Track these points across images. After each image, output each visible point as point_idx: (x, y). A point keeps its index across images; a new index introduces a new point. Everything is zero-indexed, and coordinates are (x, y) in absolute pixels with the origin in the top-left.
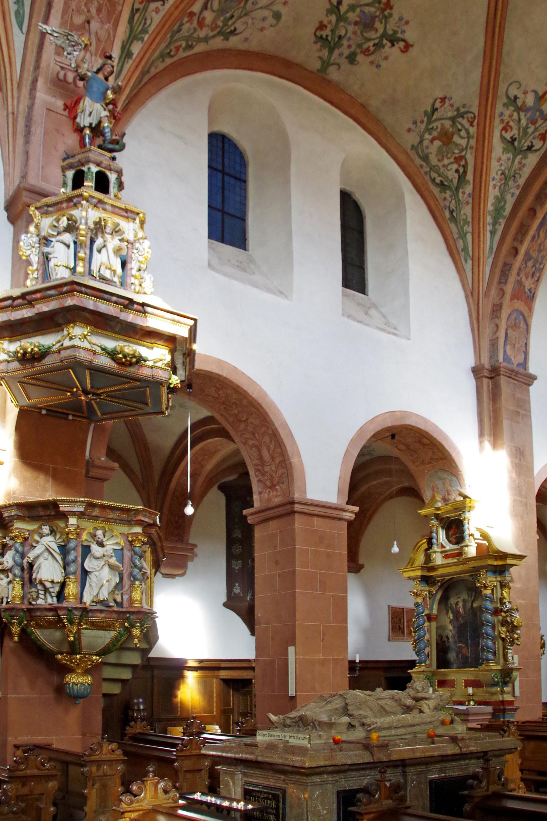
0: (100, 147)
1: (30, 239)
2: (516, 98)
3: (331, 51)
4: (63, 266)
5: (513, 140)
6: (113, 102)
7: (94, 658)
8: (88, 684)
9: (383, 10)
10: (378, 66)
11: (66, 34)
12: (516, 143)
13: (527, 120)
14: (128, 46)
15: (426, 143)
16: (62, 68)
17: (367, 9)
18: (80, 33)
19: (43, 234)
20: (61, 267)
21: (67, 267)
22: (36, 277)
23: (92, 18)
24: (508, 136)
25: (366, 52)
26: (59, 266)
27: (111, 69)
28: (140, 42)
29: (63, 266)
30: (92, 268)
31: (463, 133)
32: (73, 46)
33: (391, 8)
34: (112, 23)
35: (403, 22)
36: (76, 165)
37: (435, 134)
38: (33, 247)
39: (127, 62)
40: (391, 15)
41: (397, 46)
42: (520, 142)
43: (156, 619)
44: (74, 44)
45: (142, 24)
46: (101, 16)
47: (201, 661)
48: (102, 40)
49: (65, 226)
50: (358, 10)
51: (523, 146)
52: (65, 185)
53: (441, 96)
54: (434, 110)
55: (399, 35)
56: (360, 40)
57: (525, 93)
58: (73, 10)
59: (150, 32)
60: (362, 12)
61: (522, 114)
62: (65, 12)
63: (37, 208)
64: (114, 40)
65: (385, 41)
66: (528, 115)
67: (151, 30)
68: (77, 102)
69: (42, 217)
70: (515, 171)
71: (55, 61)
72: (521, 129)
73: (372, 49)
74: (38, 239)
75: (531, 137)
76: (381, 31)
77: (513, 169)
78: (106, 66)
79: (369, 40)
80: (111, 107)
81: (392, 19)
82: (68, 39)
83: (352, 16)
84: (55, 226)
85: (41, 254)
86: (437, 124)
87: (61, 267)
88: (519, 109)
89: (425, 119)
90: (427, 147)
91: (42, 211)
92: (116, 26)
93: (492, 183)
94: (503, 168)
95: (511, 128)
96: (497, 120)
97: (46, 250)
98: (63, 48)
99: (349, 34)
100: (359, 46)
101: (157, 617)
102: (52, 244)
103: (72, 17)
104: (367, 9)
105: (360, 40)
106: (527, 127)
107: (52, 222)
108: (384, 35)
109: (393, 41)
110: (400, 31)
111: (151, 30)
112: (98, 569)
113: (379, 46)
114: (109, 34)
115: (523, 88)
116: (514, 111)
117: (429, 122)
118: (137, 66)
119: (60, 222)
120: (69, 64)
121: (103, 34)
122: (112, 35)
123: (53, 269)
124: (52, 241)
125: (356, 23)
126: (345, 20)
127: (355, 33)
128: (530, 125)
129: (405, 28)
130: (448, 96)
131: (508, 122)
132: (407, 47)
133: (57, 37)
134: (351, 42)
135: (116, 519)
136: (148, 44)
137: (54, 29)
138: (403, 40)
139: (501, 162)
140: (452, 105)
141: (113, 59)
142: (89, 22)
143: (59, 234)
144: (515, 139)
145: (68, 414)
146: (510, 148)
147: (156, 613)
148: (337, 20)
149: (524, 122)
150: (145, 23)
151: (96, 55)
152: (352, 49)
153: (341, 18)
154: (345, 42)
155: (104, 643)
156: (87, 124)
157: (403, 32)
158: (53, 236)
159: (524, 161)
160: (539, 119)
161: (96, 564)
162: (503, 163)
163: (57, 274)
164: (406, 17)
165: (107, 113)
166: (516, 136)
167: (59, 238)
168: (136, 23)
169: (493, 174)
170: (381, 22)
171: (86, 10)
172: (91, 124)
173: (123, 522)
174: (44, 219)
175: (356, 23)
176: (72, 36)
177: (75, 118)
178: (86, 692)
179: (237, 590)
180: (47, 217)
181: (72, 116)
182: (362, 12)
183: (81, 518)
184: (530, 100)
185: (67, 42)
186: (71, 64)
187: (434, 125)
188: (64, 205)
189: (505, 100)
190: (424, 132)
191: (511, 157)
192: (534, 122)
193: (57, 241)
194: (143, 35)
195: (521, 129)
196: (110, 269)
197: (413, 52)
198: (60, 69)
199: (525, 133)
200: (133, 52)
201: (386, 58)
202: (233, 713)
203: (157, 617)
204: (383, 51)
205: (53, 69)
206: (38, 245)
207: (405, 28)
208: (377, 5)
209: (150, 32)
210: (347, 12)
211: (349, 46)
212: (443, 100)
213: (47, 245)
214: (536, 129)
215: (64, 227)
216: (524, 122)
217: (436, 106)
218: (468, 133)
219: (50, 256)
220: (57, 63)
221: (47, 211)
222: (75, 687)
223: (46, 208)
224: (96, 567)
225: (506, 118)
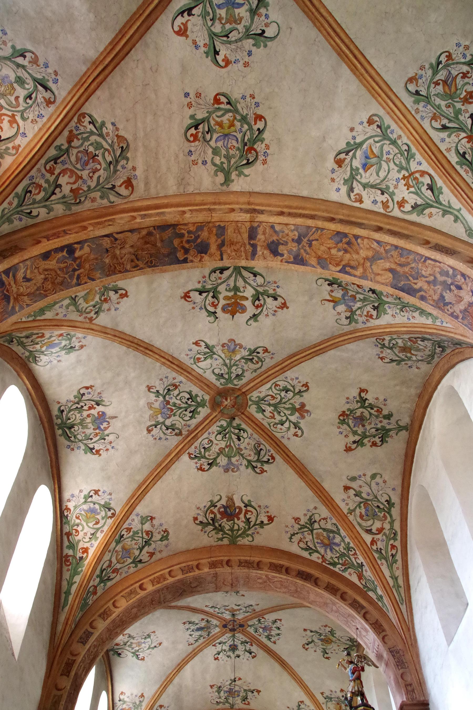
2: (347, 318)
3: (390, 430)
5: (375, 308)
9: (347, 415)
10: (385, 400)
12: (376, 305)
13: (355, 303)
15: (420, 358)
17: (352, 425)
24: (374, 313)
25: (380, 411)
31: (394, 342)
33: (344, 412)
35: (348, 401)
37: (409, 355)
40: (349, 410)
41: (365, 397)
42: (373, 302)
50: (354, 429)
51: (375, 298)
53: (380, 360)
54: (392, 361)
55: (358, 399)
56: (373, 418)
57: (339, 314)
60: (354, 426)
61: (354, 309)
65: (366, 405)
66: (352, 304)
70: (395, 299)
72: (364, 304)
73: (375, 409)
75: (365, 293)
76: (361, 410)
77: (394, 301)
79: (371, 414)
81: (351, 408)
83: (360, 430)
86: (401, 355)
88: (353, 313)
89: (403, 363)
90: (422, 357)
93: (412, 321)
94: (398, 311)
95: (368, 312)
96: (368, 325)
99: (373, 426)
100: (377, 417)
104: (352, 425)
105: (373, 418)
106: (361, 300)
108: (362, 407)
109: (363, 401)
110: (355, 400)
113: (371, 406)
115: (338, 317)
116: (356, 315)
117: (403, 360)
125: (363, 426)
126: (364, 433)
127: (370, 423)
128: (358, 299)
129: (351, 398)
130: (377, 357)
131: (365, 316)
132: (362, 391)
134: (377, 422)
138: (360, 394)
139: (394, 314)
140: (382, 352)
144: (373, 306)
146: (381, 308)
148: (366, 438)
149: (359, 305)
152: (382, 419)
153: (364, 436)
154: (379, 426)
157: (354, 397)
159: (385, 294)
160: (349, 295)
162: (394, 312)
164: (344, 401)
166: (371, 306)
169: (405, 320)
170: (356, 413)
175: (363, 426)
182: (354, 426)
184: (341, 308)
187: (403, 357)
189: (353, 324)
190: (413, 361)
191: (387, 305)
192: (354, 297)
195: (364, 304)
197: (364, 386)
199: (364, 300)
201: (377, 399)
204: (373, 403)
207: (351, 398)
208: (346, 421)
210: (359, 435)
211: (381, 422)
212: (382, 359)
214: (358, 293)
216: (359, 305)
217: (389, 361)
218: (390, 341)
225: (364, 319)
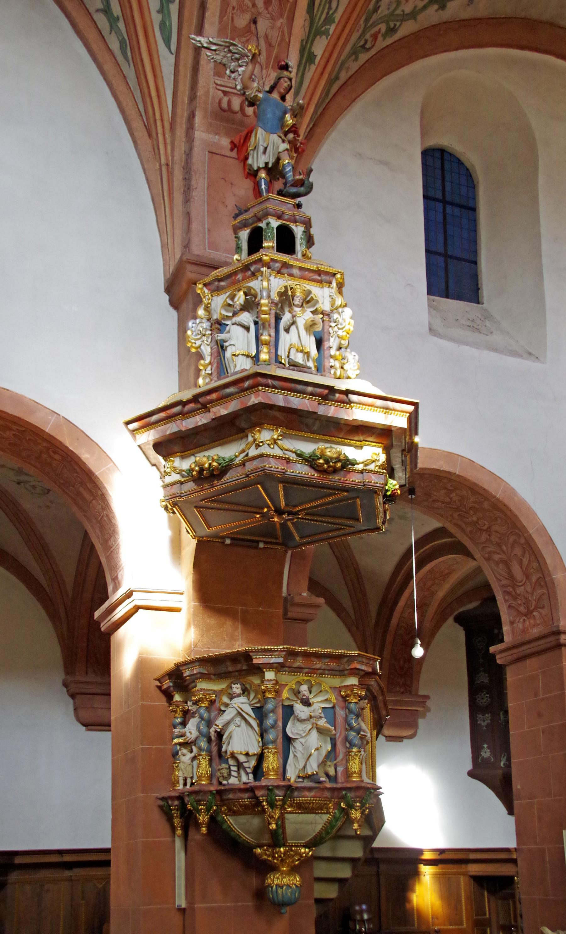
0: (280, 193)
1: (200, 325)
4: (243, 355)
6: (294, 129)
7: (303, 850)
8: (296, 886)
11: (227, 44)
14: (309, 46)
16: (225, 93)
18: (244, 39)
19: (215, 317)
20: (240, 356)
21: (248, 356)
22: (210, 372)
23: (260, 14)
26: (238, 355)
27: (289, 83)
28: (324, 37)
29: (243, 355)
30: (279, 353)
32: (238, 60)
34: (285, 18)
36: (250, 221)
38: (204, 335)
39: (309, 70)
43: (380, 796)
44: (237, 56)
45: (326, 11)
46: (270, 9)
47: (441, 851)
48: (274, 44)
49: (242, 303)
52: (238, 249)
58: (234, 8)
59: (337, 21)
62: (223, 12)
63: (205, 285)
64: (289, 42)
67: (337, 17)
68: (247, 137)
69: (212, 296)
71: (215, 85)
74: (209, 324)
78: (282, 80)
80: (291, 136)
82: (230, 51)
84: (230, 305)
85: (214, 343)
87: (240, 356)
91: (213, 287)
92: (291, 20)
97: (221, 336)
98: (224, 65)
101: (382, 793)
102: (228, 328)
103: (232, 18)
107: (225, 300)
111: (337, 17)
112: (304, 735)
114: (283, 34)
118: (322, 73)
119: (236, 299)
120: (233, 86)
121: (274, 36)
122: (286, 35)
123: (230, 360)
124: (227, 325)
133: (215, 50)
136: (335, 37)
137: (211, 40)
141: (290, 69)
142: (255, 22)
143: (235, 314)
145: (258, 542)
147: (380, 788)
150: (330, 8)
151: (267, 67)
155: (314, 831)
156: (262, 165)
158: (228, 318)
161: (301, 729)
163: (235, 366)
165: (286, 146)
167: (235, 319)
168: (317, 11)
171: (250, 5)
172: (267, 164)
174: (214, 298)
176: (235, 45)
177: (246, 158)
178: (293, 897)
179: (486, 753)
180: (218, 295)
181: (242, 157)
185: (229, 55)
186: (236, 85)
188: (240, 276)
193: (233, 324)
194: (328, 27)
196: (302, 351)
198: (222, 95)
200: (315, 54)
202: (490, 927)
203: (382, 793)
205: (213, 97)
206: (210, 332)
209: (337, 21)
213: (220, 331)
215: (241, 304)
219: (226, 344)
220: (219, 87)
221: (218, 287)
222: (280, 891)
223: (217, 283)
224: (301, 732)
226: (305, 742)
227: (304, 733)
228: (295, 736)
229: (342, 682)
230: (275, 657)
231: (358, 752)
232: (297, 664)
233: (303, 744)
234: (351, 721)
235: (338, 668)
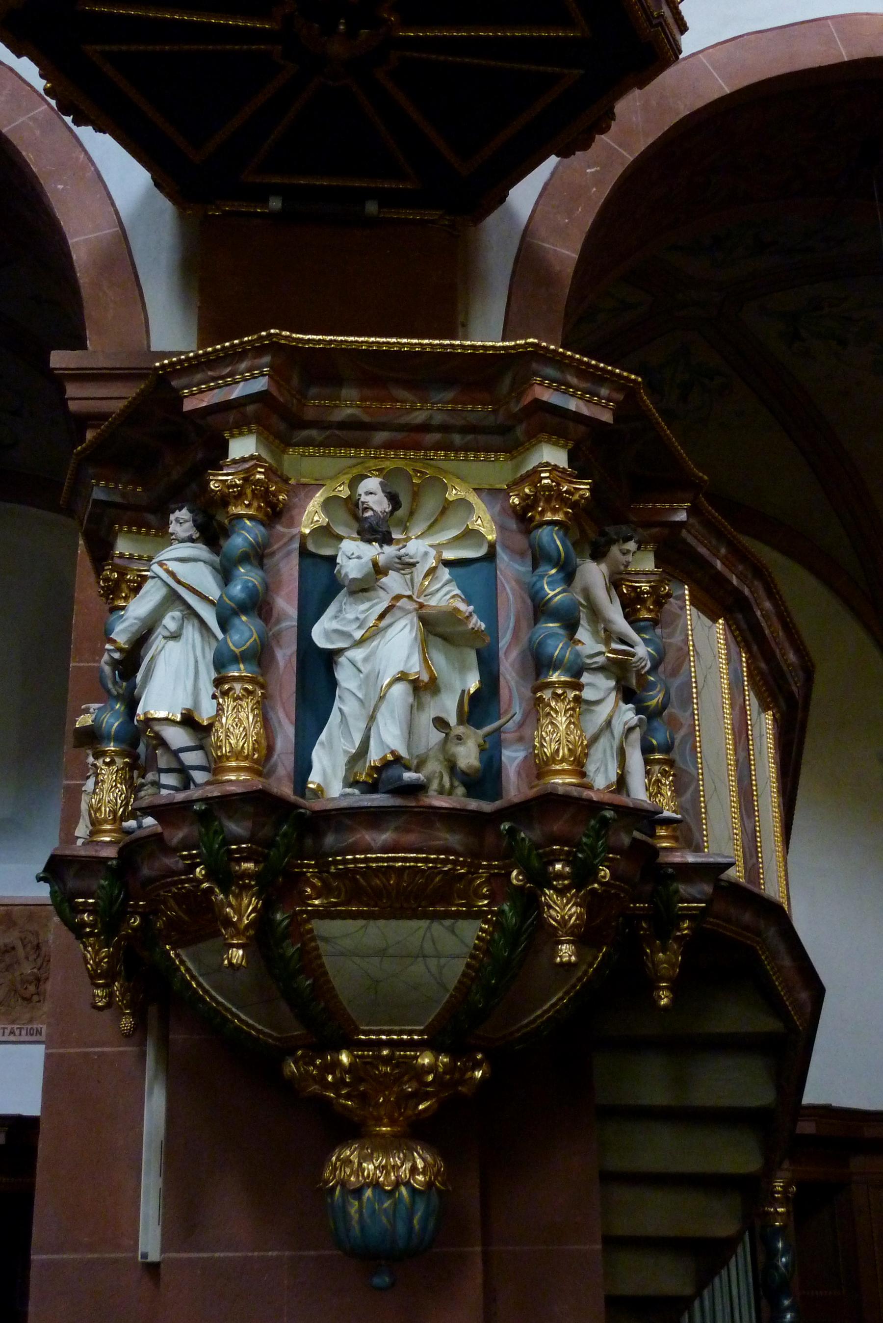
112: (358, 635)
135: (444, 428)
161: (350, 616)
173: (482, 439)
183: (289, 444)
224: (350, 628)
226: (366, 660)
227: (359, 627)
228: (332, 643)
229: (518, 467)
230: (245, 380)
231: (564, 684)
232: (346, 412)
233: (360, 665)
234: (538, 585)
235: (491, 420)
